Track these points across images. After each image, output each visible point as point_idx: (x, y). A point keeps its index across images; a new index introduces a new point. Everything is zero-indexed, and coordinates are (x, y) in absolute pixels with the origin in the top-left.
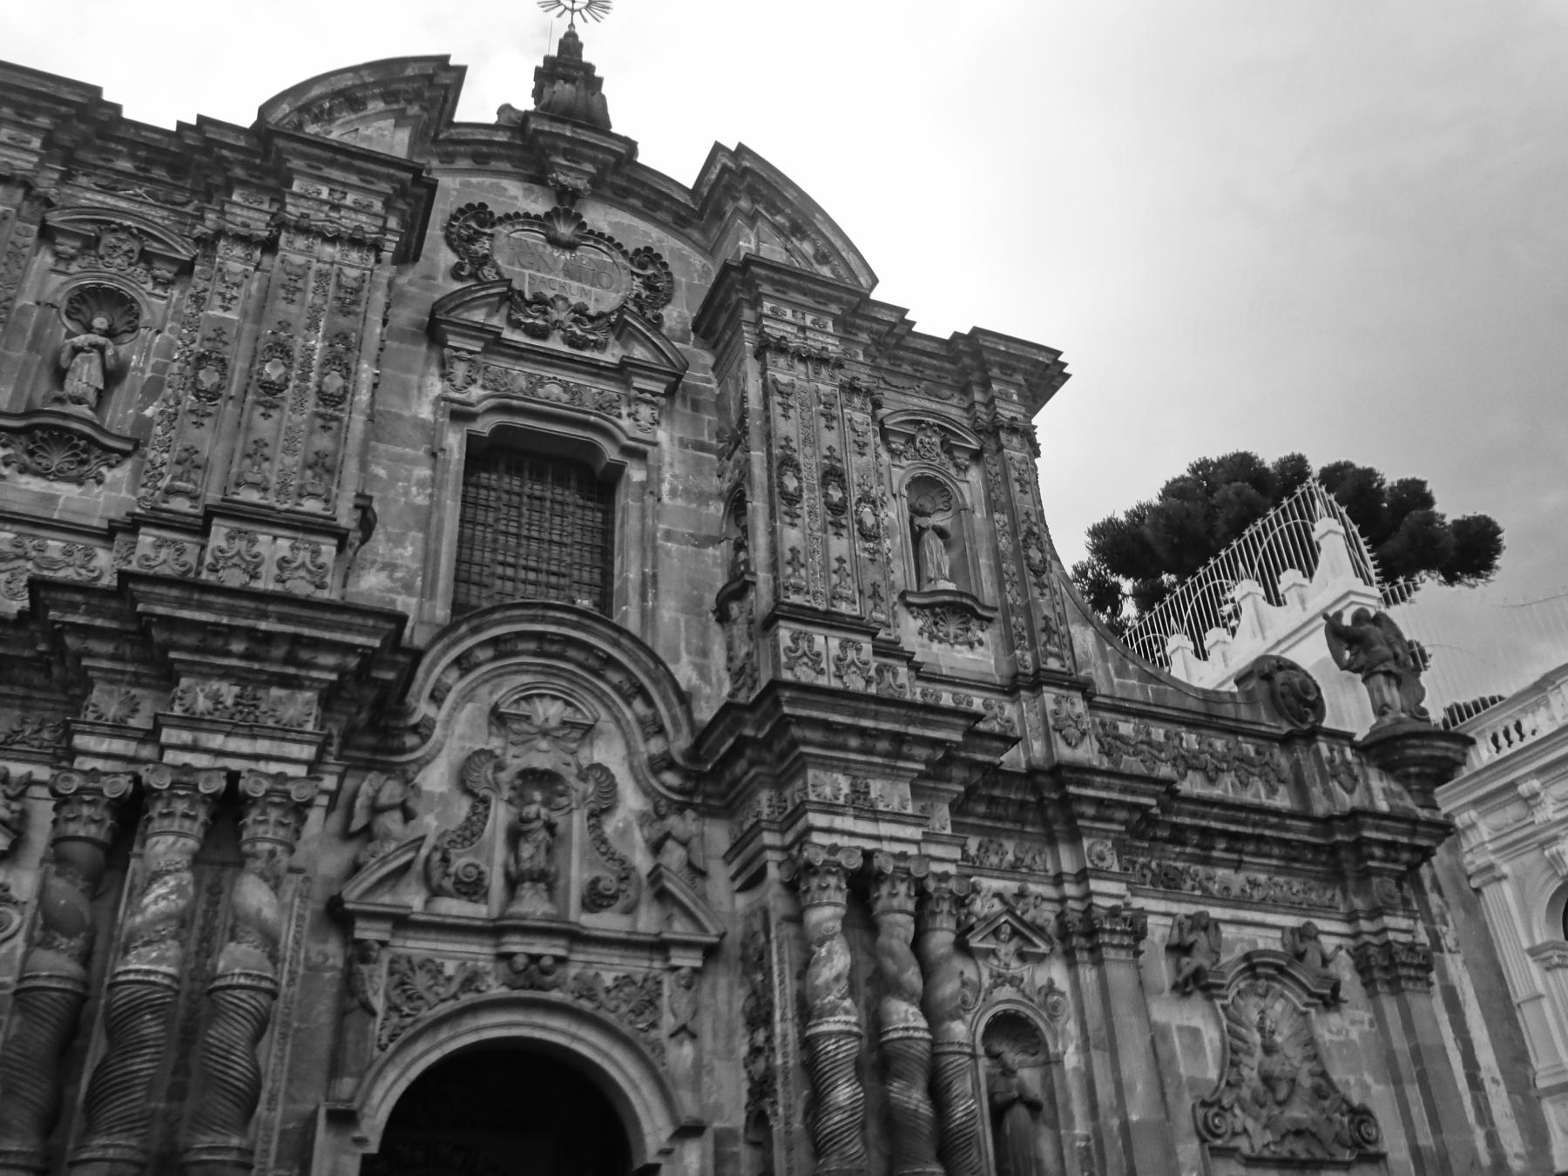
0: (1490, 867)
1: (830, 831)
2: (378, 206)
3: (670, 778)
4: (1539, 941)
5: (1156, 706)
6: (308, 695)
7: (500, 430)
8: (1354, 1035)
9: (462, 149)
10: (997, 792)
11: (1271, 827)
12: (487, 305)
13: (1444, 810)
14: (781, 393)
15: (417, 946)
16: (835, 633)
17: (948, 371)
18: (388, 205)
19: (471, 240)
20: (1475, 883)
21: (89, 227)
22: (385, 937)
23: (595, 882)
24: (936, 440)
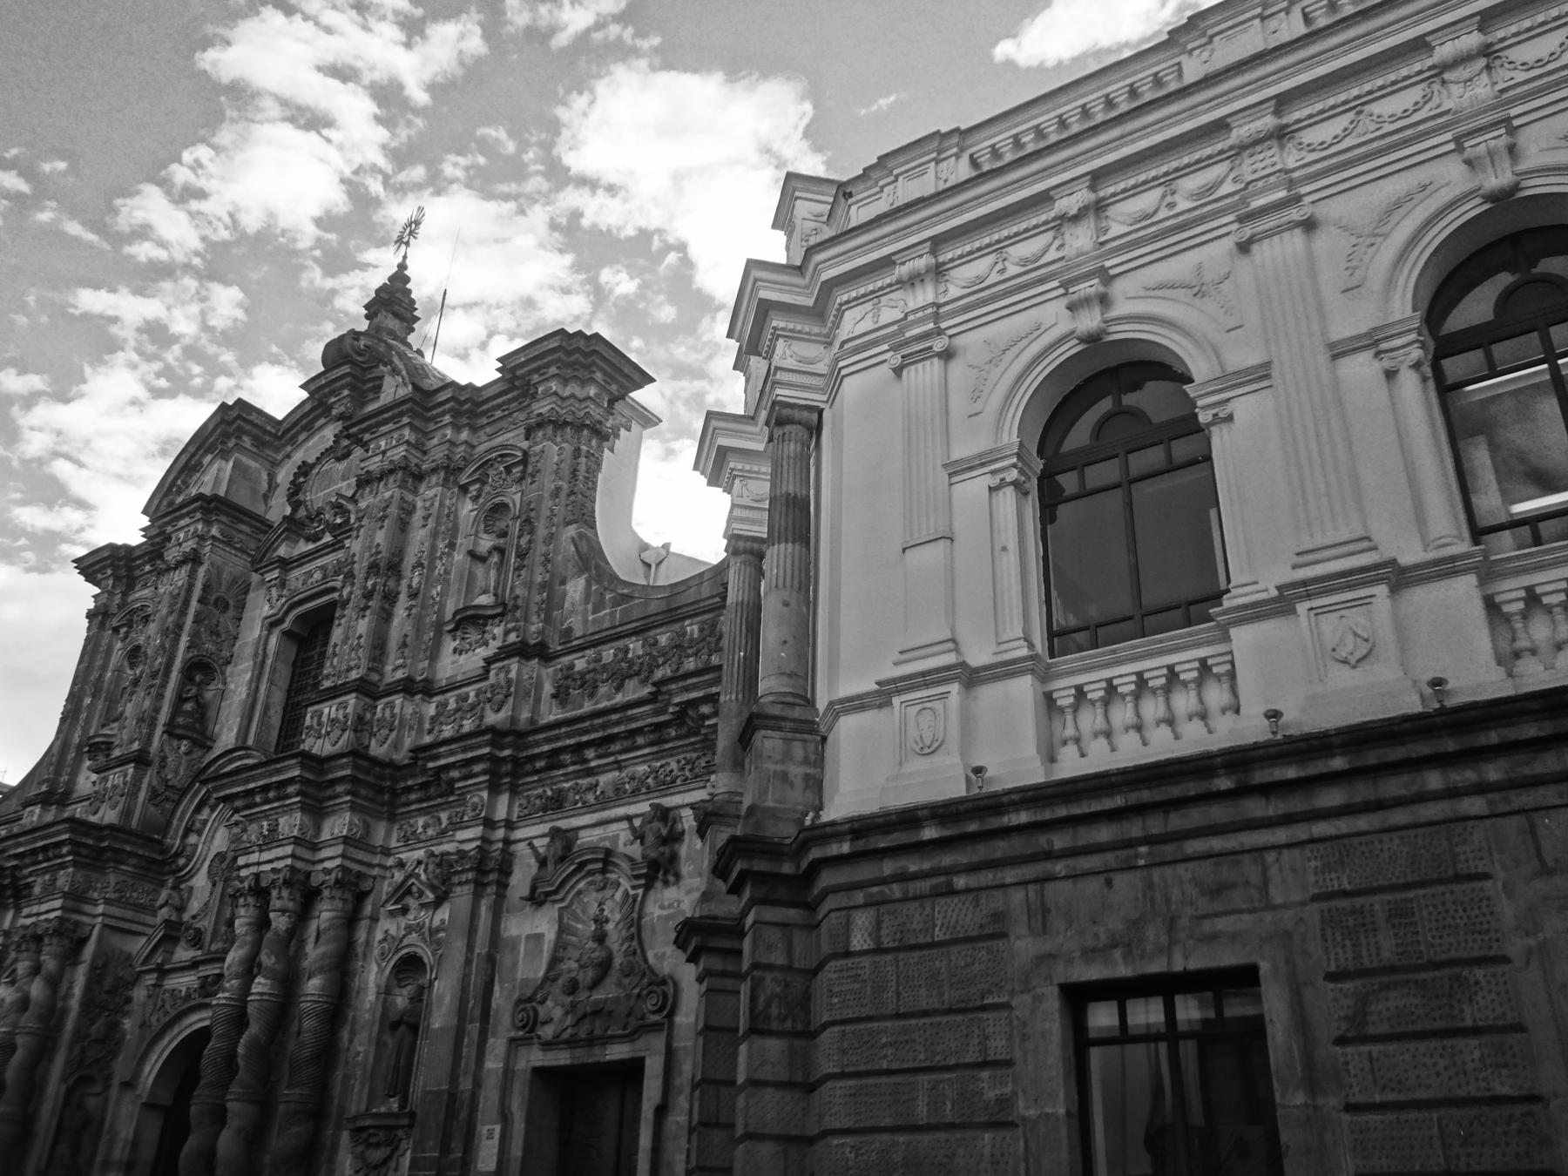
1: (247, 866)
2: (200, 526)
5: (621, 625)
6: (71, 870)
7: (299, 618)
9: (294, 431)
10: (410, 783)
11: (618, 723)
12: (284, 540)
15: (173, 982)
18: (208, 523)
19: (295, 493)
22: (153, 982)
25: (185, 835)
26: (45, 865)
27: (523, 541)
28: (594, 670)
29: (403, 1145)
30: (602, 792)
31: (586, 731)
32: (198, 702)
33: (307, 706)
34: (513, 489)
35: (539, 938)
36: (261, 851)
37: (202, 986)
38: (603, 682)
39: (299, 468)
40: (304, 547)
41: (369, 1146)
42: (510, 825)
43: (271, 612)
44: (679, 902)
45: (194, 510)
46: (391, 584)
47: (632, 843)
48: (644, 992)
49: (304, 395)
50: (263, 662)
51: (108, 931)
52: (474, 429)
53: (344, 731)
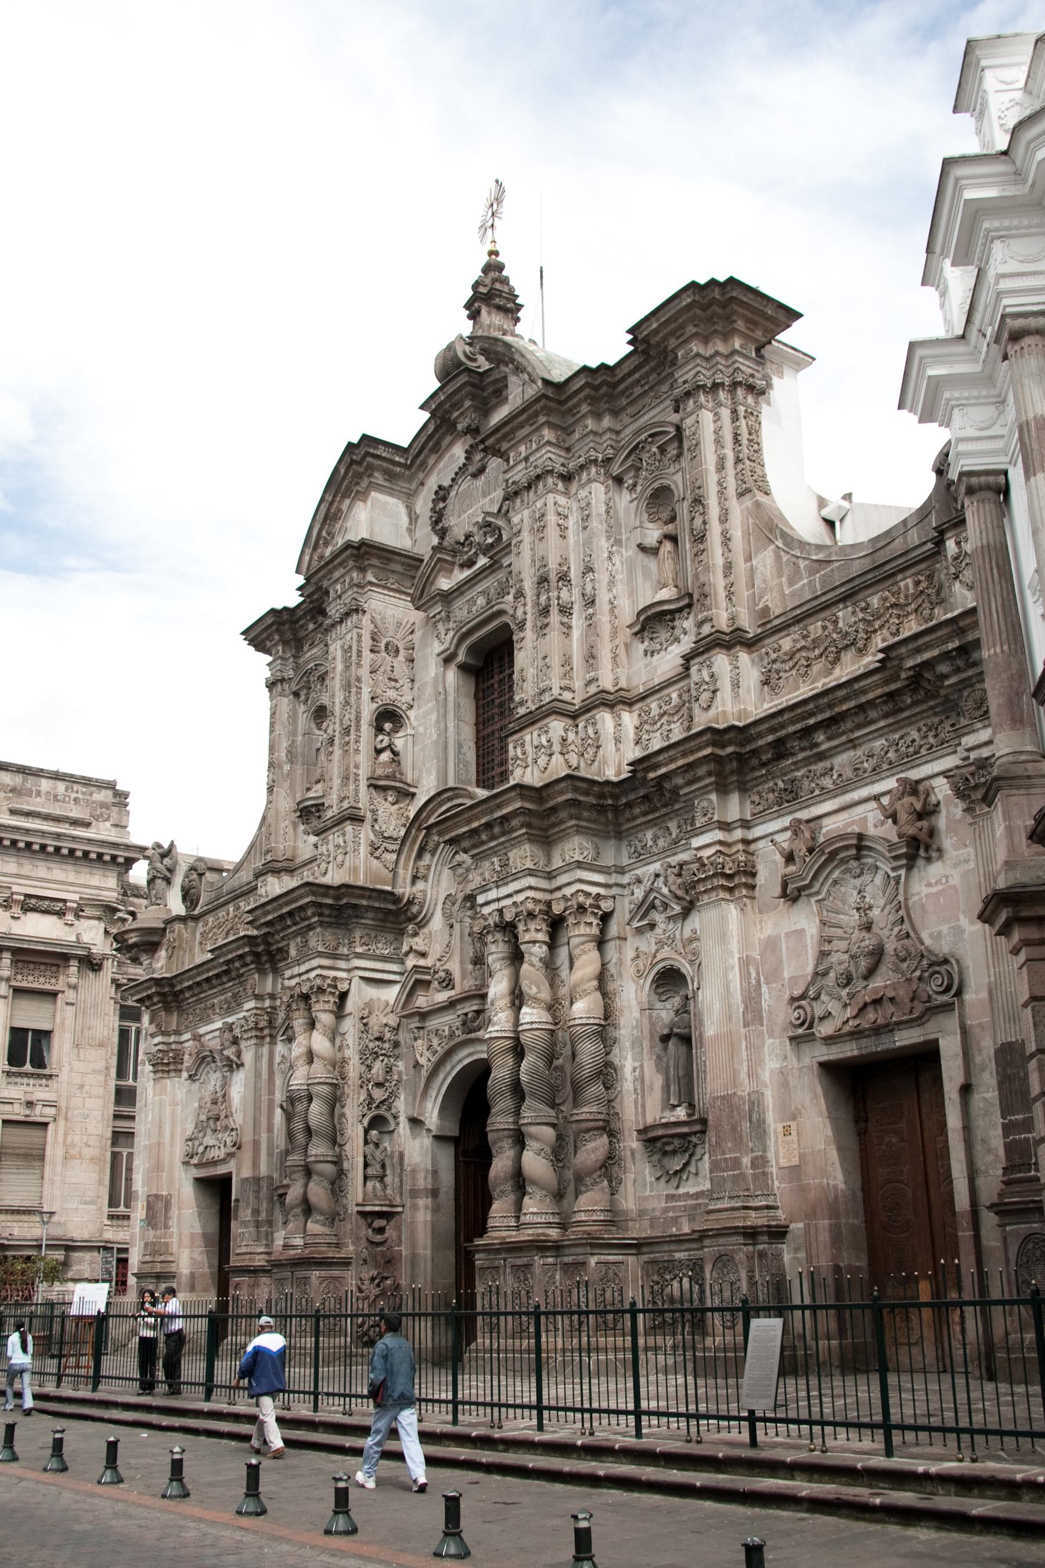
1: (487, 903)
2: (355, 574)
6: (319, 930)
7: (471, 650)
8: (955, 880)
15: (433, 1023)
17: (658, 365)
18: (363, 570)
19: (436, 523)
24: (654, 449)
25: (413, 883)
26: (294, 928)
27: (698, 522)
28: (803, 648)
29: (699, 1151)
30: (840, 775)
31: (812, 714)
32: (393, 752)
33: (507, 737)
34: (672, 470)
35: (801, 933)
36: (498, 887)
37: (464, 1024)
38: (816, 658)
39: (436, 493)
40: (461, 575)
41: (665, 1153)
42: (746, 824)
43: (442, 648)
44: (947, 877)
46: (564, 594)
47: (883, 823)
48: (926, 974)
49: (426, 415)
50: (446, 699)
51: (363, 984)
52: (616, 413)
53: (550, 755)
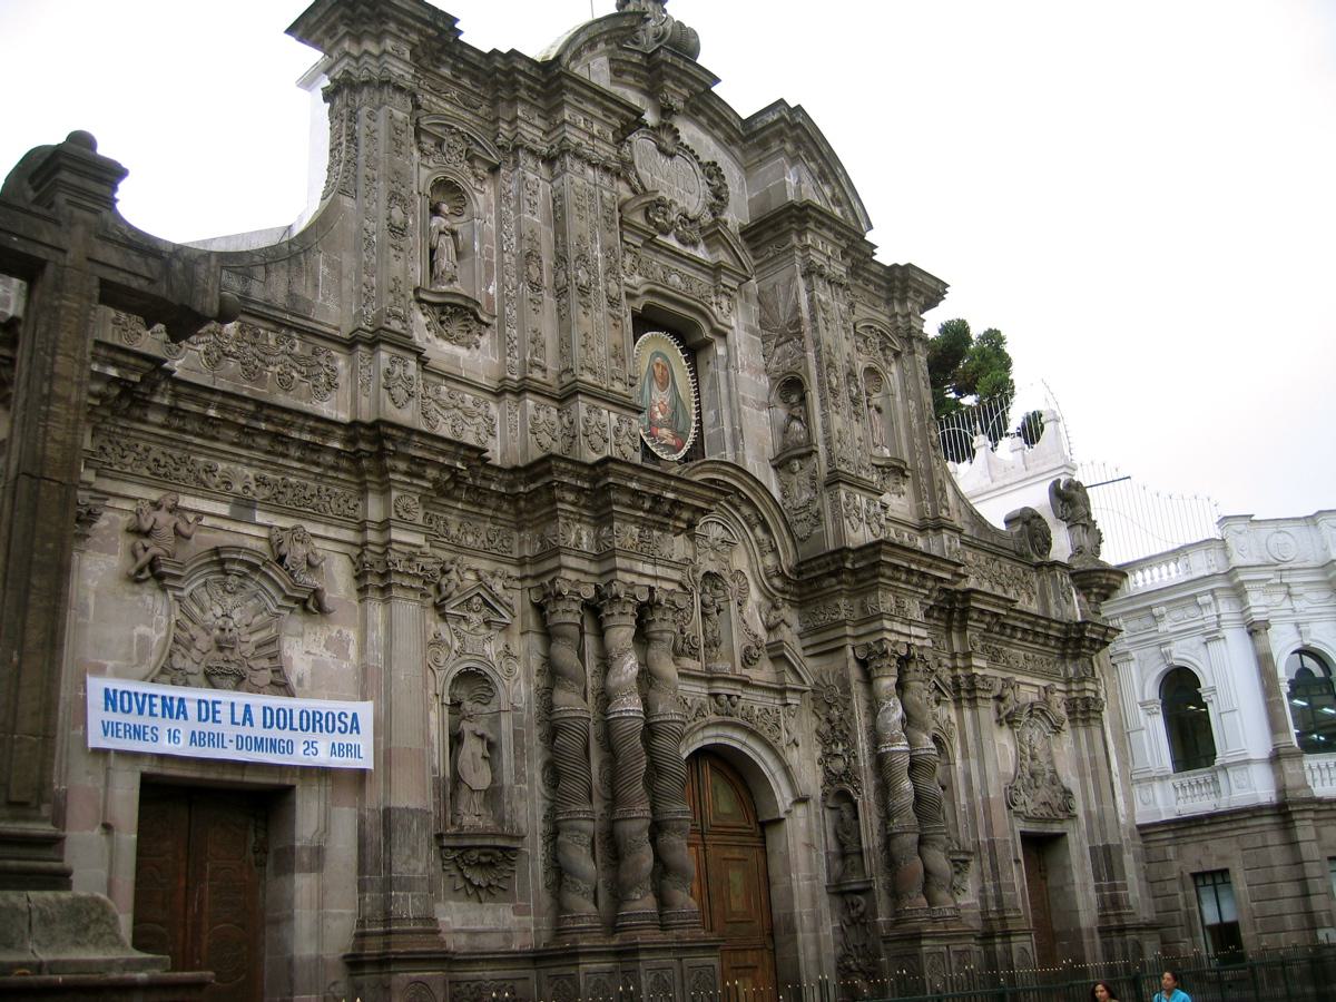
0: (1127, 653)
1: (891, 631)
3: (777, 582)
4: (1147, 699)
7: (647, 307)
13: (1103, 615)
14: (823, 309)
16: (866, 494)
20: (1114, 660)
21: (439, 130)
23: (748, 648)
45: (614, 113)
